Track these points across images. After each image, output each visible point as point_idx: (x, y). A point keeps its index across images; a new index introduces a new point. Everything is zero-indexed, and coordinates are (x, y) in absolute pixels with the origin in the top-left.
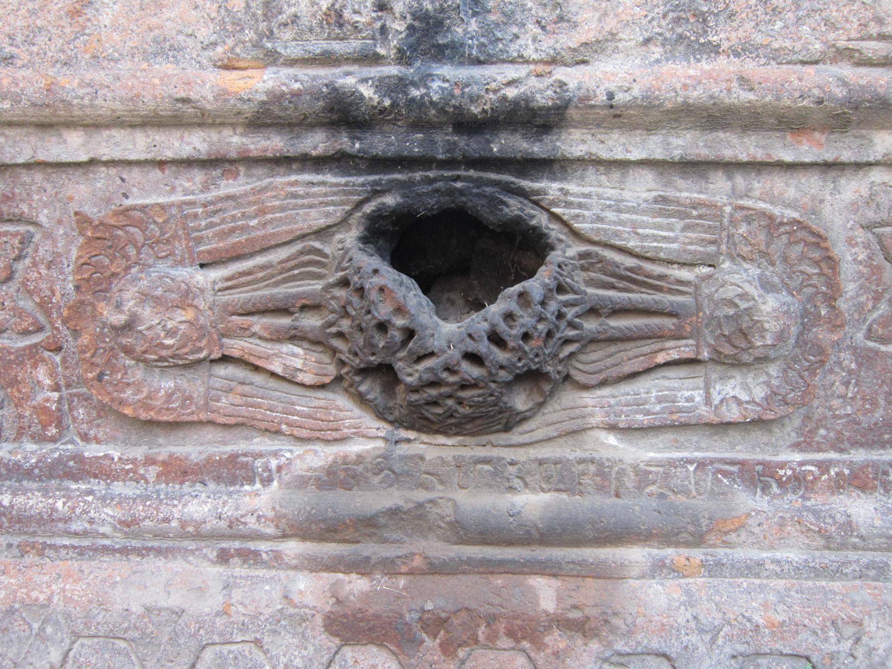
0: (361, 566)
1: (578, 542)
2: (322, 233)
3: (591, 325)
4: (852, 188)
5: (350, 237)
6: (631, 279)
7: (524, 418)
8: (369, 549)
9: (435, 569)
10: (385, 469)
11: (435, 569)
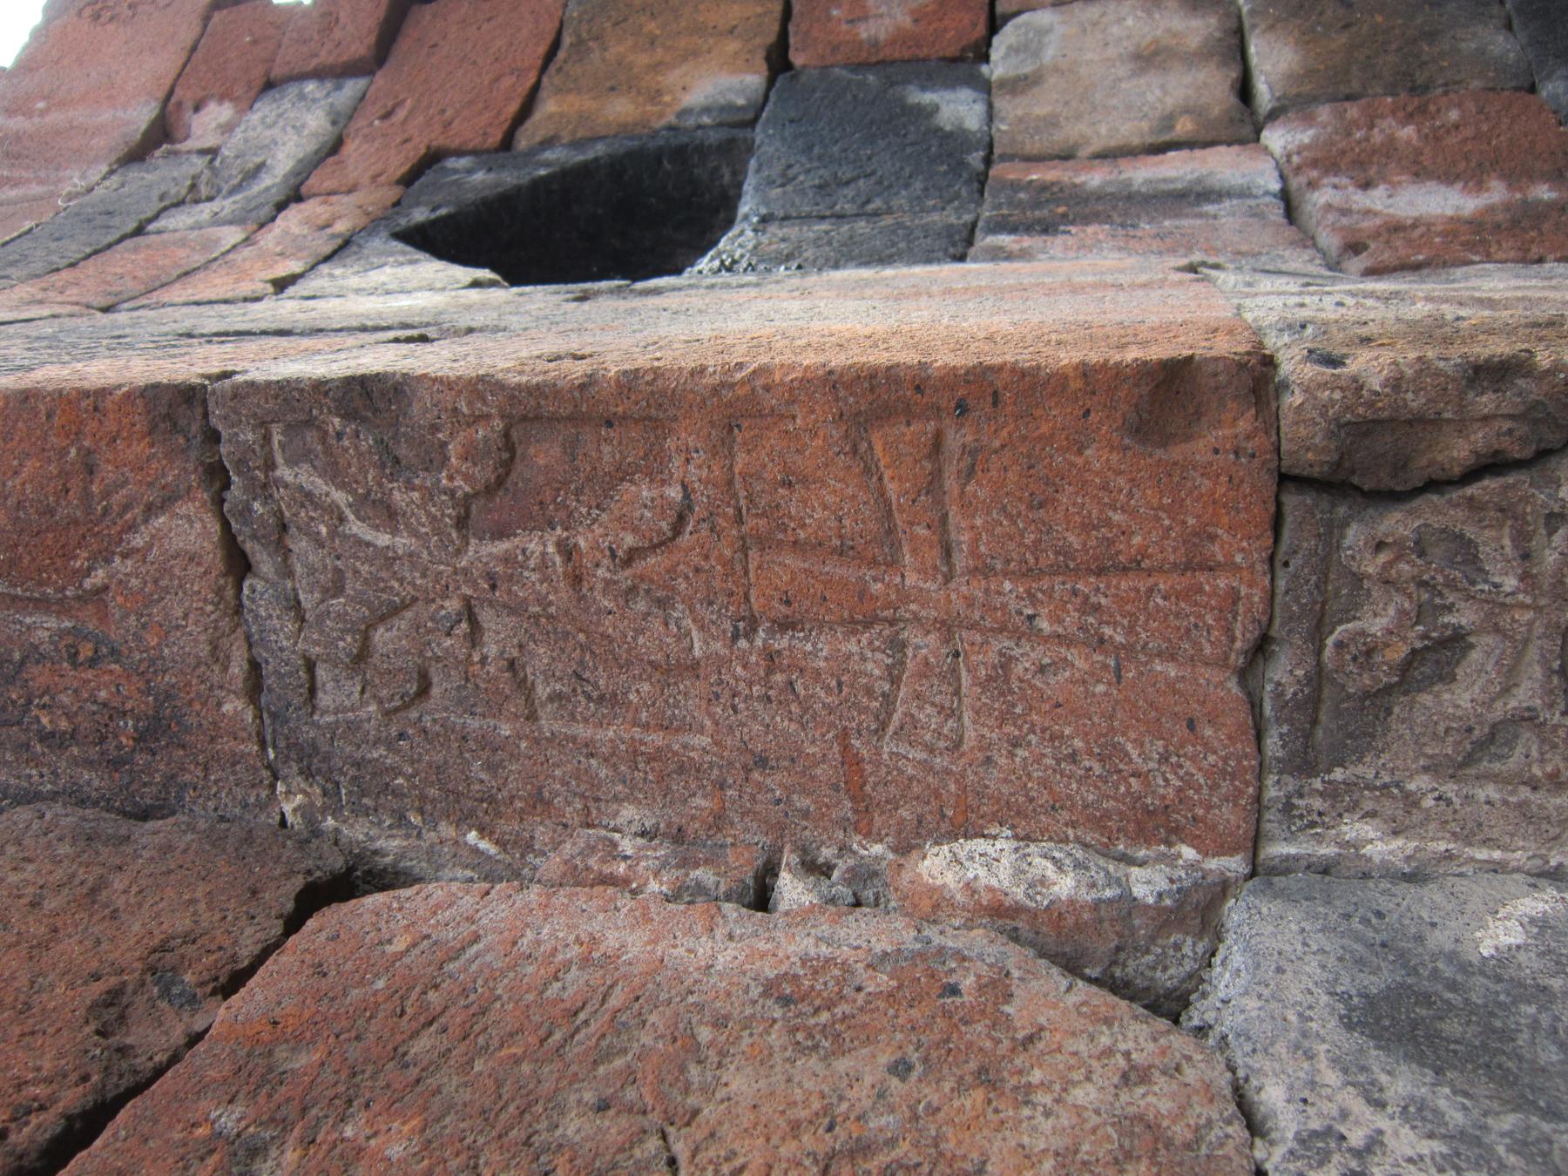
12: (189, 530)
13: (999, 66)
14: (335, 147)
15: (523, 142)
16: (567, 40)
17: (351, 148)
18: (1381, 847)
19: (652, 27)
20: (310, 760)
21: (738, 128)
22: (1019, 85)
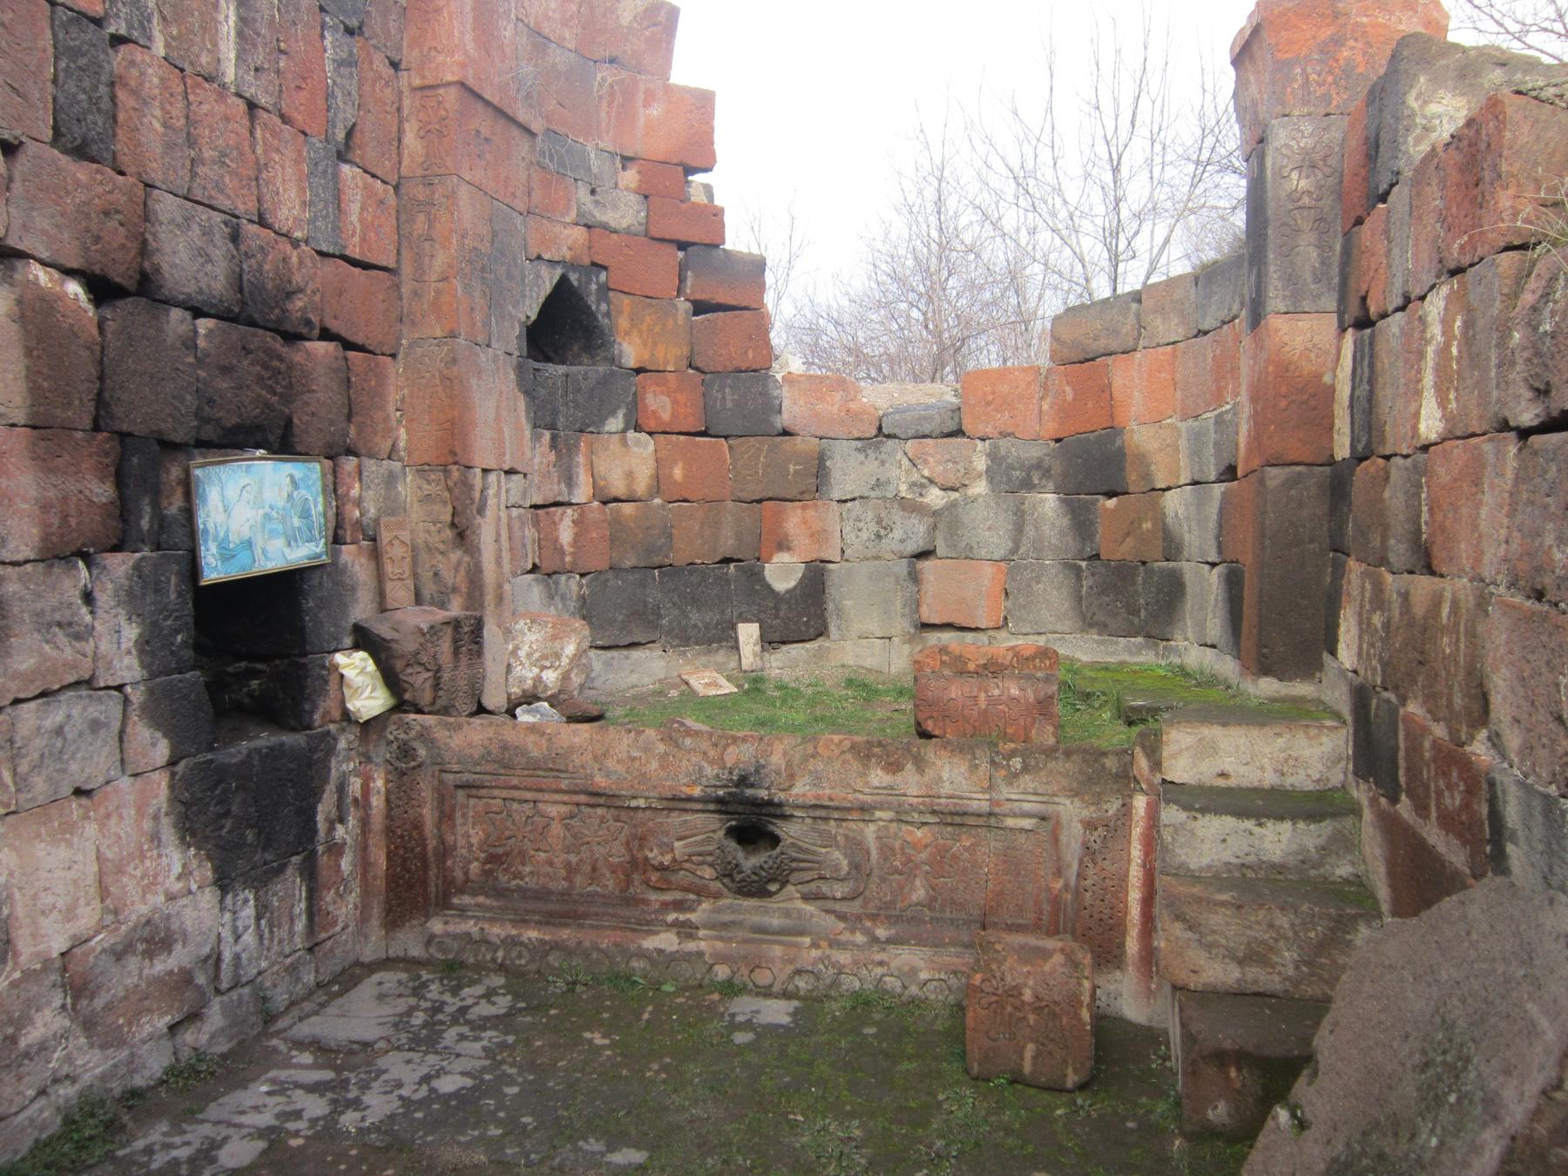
0: (720, 938)
1: (789, 934)
2: (714, 831)
3: (794, 865)
4: (872, 827)
5: (722, 833)
6: (806, 851)
7: (775, 893)
8: (724, 933)
9: (745, 941)
10: (730, 907)
11: (745, 941)
12: (438, 333)
13: (631, 434)
14: (615, 232)
15: (611, 294)
16: (654, 302)
17: (614, 236)
18: (409, 479)
19: (657, 329)
20: (410, 346)
21: (612, 360)
22: (624, 442)
